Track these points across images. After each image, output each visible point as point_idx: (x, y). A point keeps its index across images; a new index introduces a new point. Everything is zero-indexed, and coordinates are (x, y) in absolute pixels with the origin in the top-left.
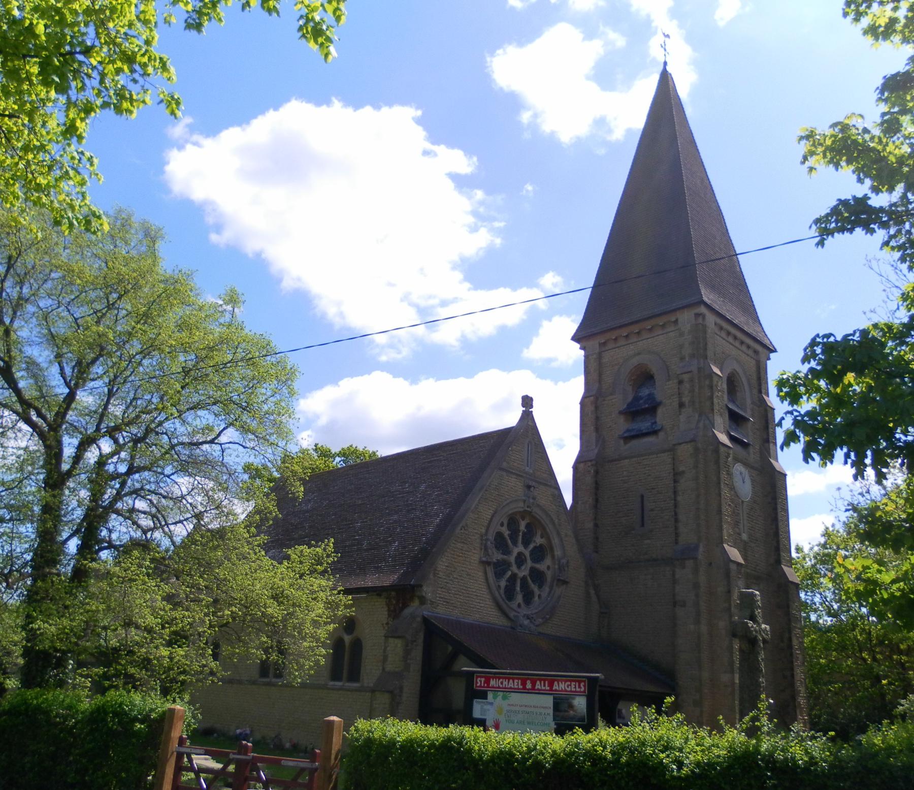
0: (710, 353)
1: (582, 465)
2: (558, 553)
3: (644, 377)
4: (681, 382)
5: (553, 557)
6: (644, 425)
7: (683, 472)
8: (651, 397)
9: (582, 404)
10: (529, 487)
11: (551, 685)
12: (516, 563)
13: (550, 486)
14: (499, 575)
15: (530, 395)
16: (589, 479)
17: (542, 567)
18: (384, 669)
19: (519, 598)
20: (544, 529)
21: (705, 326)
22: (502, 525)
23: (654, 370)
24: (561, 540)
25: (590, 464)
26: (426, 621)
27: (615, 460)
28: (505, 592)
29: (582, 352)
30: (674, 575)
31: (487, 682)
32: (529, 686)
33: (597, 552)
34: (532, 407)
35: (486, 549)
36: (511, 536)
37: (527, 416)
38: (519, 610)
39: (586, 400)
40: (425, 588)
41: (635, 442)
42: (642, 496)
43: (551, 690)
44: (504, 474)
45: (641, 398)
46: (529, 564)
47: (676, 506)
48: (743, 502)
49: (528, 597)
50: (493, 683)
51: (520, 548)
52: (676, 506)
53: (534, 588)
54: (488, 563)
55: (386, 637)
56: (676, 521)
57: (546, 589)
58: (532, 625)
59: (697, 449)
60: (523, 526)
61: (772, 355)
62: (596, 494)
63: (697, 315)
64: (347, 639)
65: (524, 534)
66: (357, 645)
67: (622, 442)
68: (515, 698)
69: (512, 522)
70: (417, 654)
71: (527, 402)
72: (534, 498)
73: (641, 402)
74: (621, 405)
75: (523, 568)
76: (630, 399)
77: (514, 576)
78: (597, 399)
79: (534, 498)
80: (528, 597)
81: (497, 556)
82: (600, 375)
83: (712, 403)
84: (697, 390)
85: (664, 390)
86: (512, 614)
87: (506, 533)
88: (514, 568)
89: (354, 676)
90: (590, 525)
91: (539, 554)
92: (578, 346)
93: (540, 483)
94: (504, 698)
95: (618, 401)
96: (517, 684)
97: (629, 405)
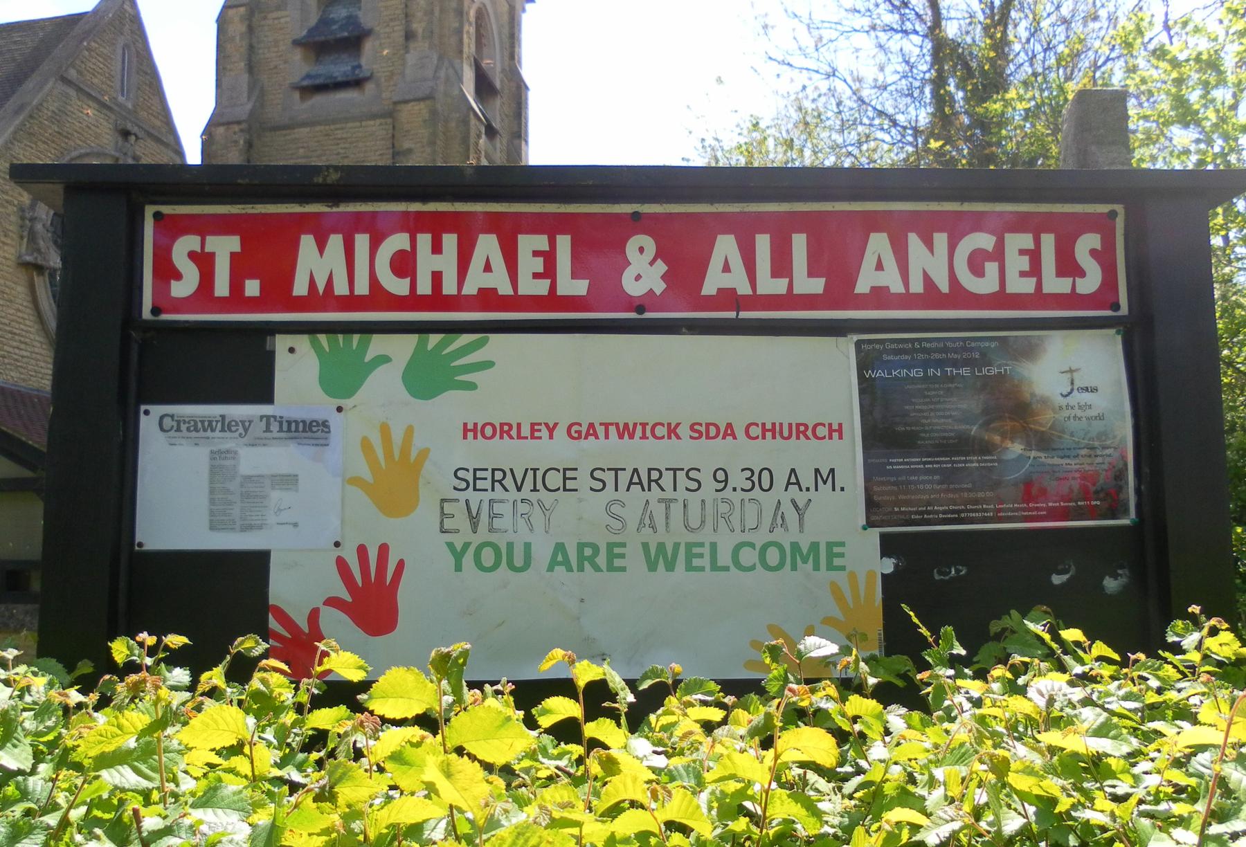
1: (221, 130)
6: (339, 68)
7: (410, 151)
8: (352, 21)
9: (222, 22)
10: (126, 134)
13: (166, 145)
25: (236, 128)
39: (231, 12)
41: (319, 99)
45: (334, 22)
54: (39, 269)
59: (434, 113)
67: (297, 95)
73: (334, 27)
76: (313, 20)
83: (461, 41)
84: (437, 13)
93: (150, 135)
97: (311, 31)
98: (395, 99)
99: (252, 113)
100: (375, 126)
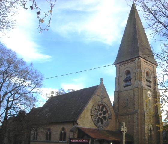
3: (128, 73)
4: (135, 74)
5: (108, 113)
6: (128, 83)
8: (130, 77)
10: (102, 98)
13: (107, 98)
15: (102, 78)
16: (117, 96)
17: (105, 116)
19: (100, 122)
20: (106, 107)
21: (140, 62)
23: (131, 71)
24: (110, 110)
30: (133, 116)
34: (103, 80)
40: (78, 121)
42: (128, 99)
46: (102, 115)
49: (102, 122)
51: (100, 112)
55: (70, 132)
58: (103, 128)
61: (157, 67)
64: (63, 132)
66: (65, 133)
67: (124, 87)
71: (102, 79)
76: (125, 78)
77: (99, 118)
80: (102, 122)
82: (119, 72)
85: (132, 76)
88: (99, 116)
89: (64, 140)
90: (117, 106)
91: (105, 113)
92: (115, 66)
97: (126, 79)
100: (132, 91)
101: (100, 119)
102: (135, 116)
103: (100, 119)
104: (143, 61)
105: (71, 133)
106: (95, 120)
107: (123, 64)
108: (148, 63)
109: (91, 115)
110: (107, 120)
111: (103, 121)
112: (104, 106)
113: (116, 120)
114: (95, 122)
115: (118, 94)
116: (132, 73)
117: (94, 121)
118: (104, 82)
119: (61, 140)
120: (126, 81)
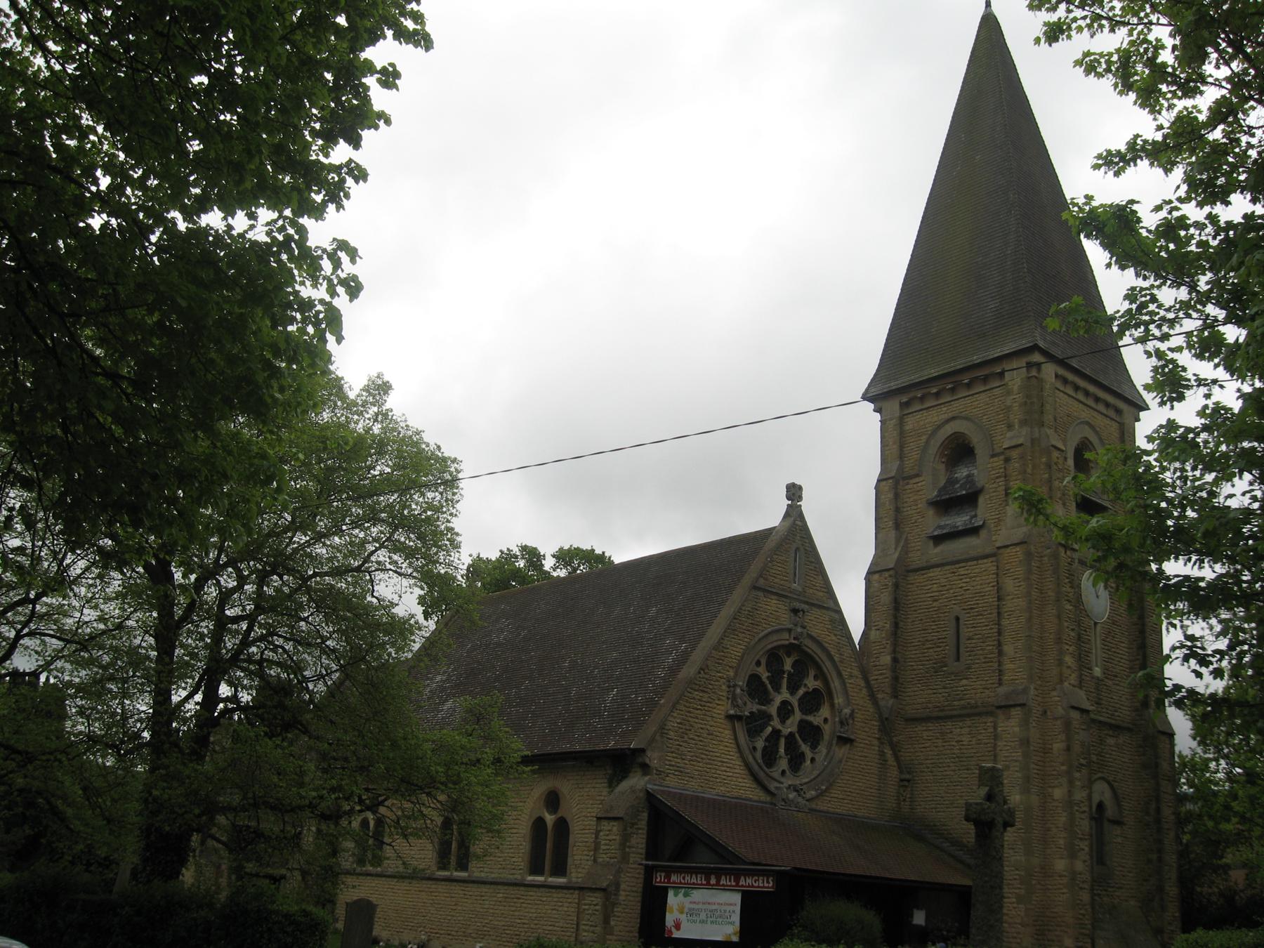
0: (1048, 418)
1: (876, 577)
2: (839, 700)
3: (960, 451)
4: (1007, 460)
5: (832, 706)
6: (960, 520)
10: (795, 611)
11: (737, 881)
12: (779, 715)
14: (753, 733)
15: (798, 483)
16: (886, 598)
17: (816, 720)
18: (595, 861)
19: (783, 764)
20: (818, 667)
21: (1040, 380)
22: (758, 663)
23: (976, 440)
24: (843, 683)
25: (887, 574)
26: (650, 796)
27: (922, 569)
28: (763, 756)
29: (878, 416)
30: (995, 728)
31: (668, 877)
32: (713, 881)
33: (896, 697)
34: (800, 498)
35: (734, 698)
36: (770, 679)
37: (794, 515)
38: (782, 780)
40: (649, 753)
42: (957, 619)
43: (737, 885)
44: (760, 594)
45: (957, 481)
46: (798, 716)
47: (999, 633)
48: (1096, 624)
49: (796, 761)
50: (674, 878)
52: (999, 633)
53: (805, 748)
56: (1000, 653)
57: (822, 749)
58: (800, 800)
59: (1029, 555)
60: (788, 665)
61: (1142, 414)
62: (895, 617)
63: (1030, 365)
65: (790, 674)
68: (697, 895)
69: (774, 658)
70: (639, 841)
71: (794, 492)
72: (804, 627)
74: (929, 487)
75: (789, 722)
76: (942, 482)
77: (776, 733)
78: (897, 483)
79: (804, 627)
80: (796, 761)
81: (753, 707)
82: (901, 447)
86: (772, 786)
87: (765, 675)
88: (776, 723)
89: (560, 868)
90: (887, 659)
91: (812, 701)
92: (872, 406)
94: (686, 895)
95: (927, 487)
96: (699, 879)
98: (998, 544)
99: (899, 560)
100: (988, 565)
101: (782, 741)
102: (1011, 726)
103: (782, 741)
104: (1057, 376)
105: (606, 826)
106: (755, 748)
107: (922, 399)
108: (1087, 393)
109: (730, 718)
110: (824, 751)
111: (803, 755)
112: (805, 662)
113: (882, 754)
114: (751, 759)
115: (888, 581)
116: (981, 452)
117: (747, 753)
118: (806, 506)
119: (536, 868)
120: (945, 505)
